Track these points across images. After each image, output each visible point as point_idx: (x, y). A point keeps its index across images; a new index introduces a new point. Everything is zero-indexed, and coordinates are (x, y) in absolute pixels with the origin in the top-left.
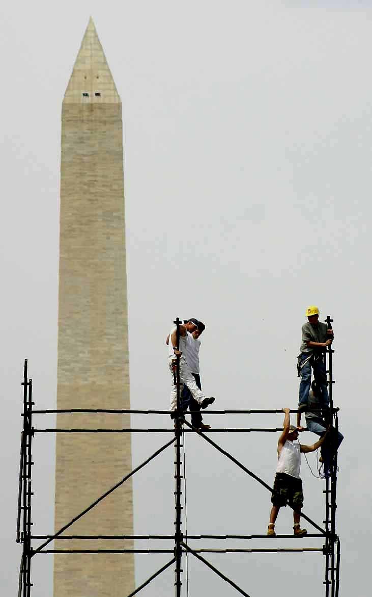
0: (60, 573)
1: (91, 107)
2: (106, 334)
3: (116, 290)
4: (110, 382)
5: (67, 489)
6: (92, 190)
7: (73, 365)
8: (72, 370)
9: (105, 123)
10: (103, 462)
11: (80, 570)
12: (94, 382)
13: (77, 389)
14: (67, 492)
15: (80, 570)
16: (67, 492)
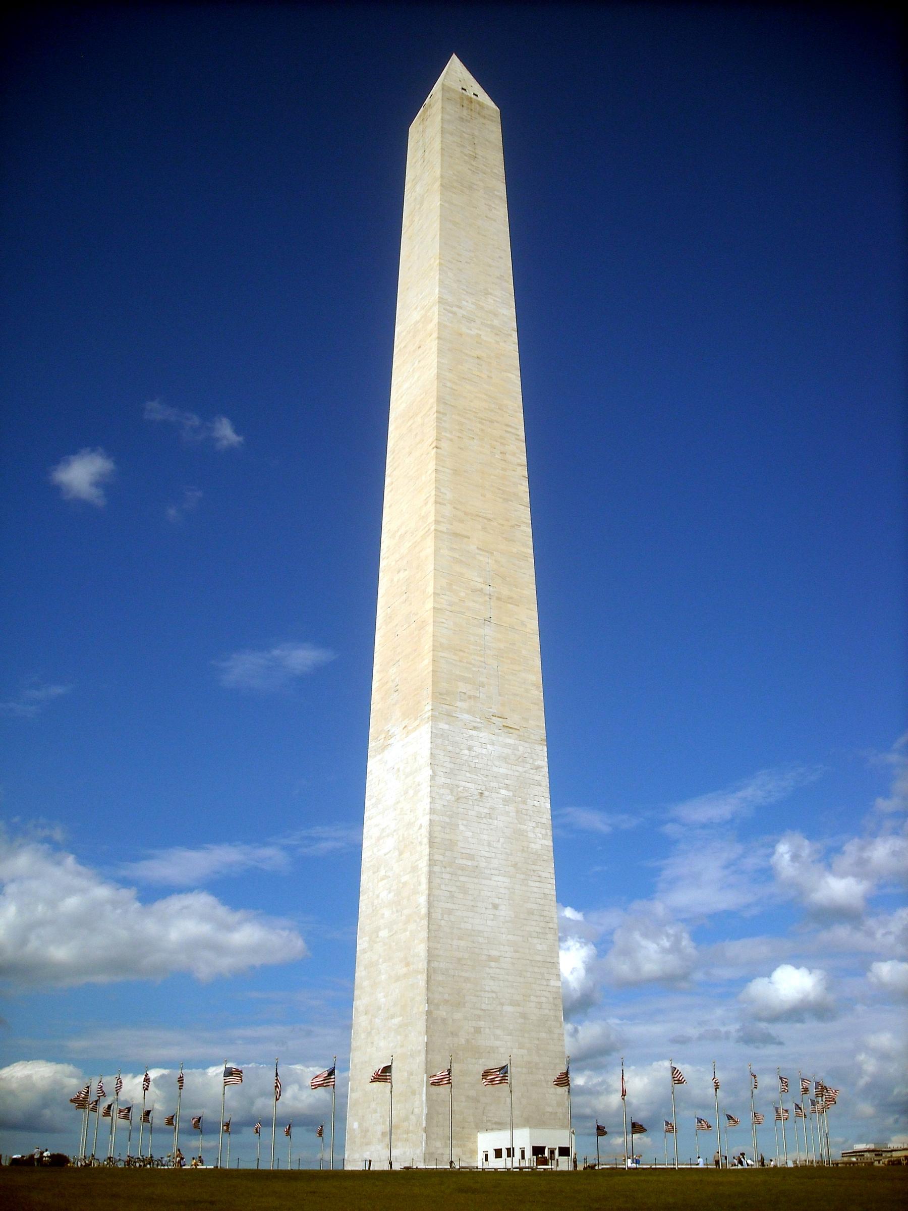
0: (441, 532)
1: (471, 101)
2: (491, 294)
3: (500, 257)
4: (498, 343)
5: (448, 435)
6: (474, 163)
7: (455, 309)
8: (454, 313)
9: (484, 117)
10: (492, 422)
11: (469, 538)
12: (479, 336)
13: (461, 335)
14: (451, 440)
15: (469, 538)
16: (451, 440)
